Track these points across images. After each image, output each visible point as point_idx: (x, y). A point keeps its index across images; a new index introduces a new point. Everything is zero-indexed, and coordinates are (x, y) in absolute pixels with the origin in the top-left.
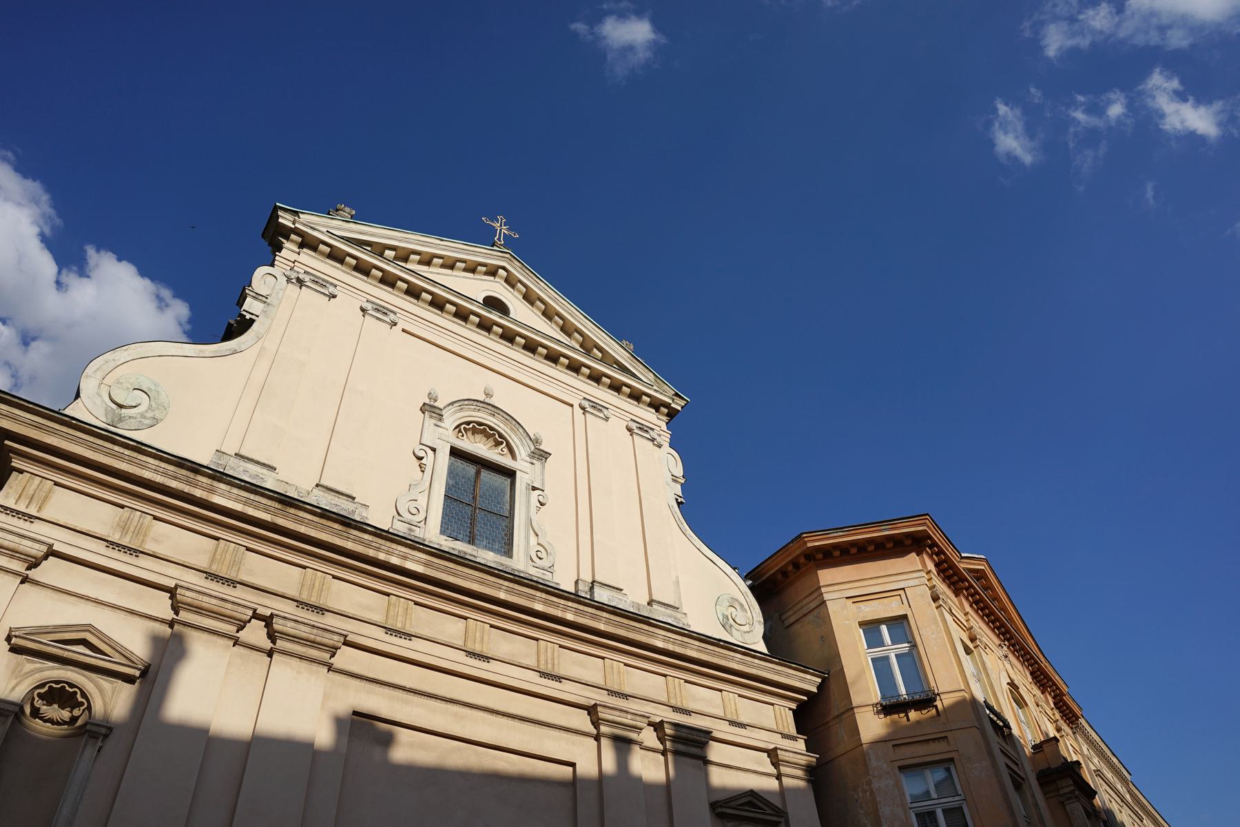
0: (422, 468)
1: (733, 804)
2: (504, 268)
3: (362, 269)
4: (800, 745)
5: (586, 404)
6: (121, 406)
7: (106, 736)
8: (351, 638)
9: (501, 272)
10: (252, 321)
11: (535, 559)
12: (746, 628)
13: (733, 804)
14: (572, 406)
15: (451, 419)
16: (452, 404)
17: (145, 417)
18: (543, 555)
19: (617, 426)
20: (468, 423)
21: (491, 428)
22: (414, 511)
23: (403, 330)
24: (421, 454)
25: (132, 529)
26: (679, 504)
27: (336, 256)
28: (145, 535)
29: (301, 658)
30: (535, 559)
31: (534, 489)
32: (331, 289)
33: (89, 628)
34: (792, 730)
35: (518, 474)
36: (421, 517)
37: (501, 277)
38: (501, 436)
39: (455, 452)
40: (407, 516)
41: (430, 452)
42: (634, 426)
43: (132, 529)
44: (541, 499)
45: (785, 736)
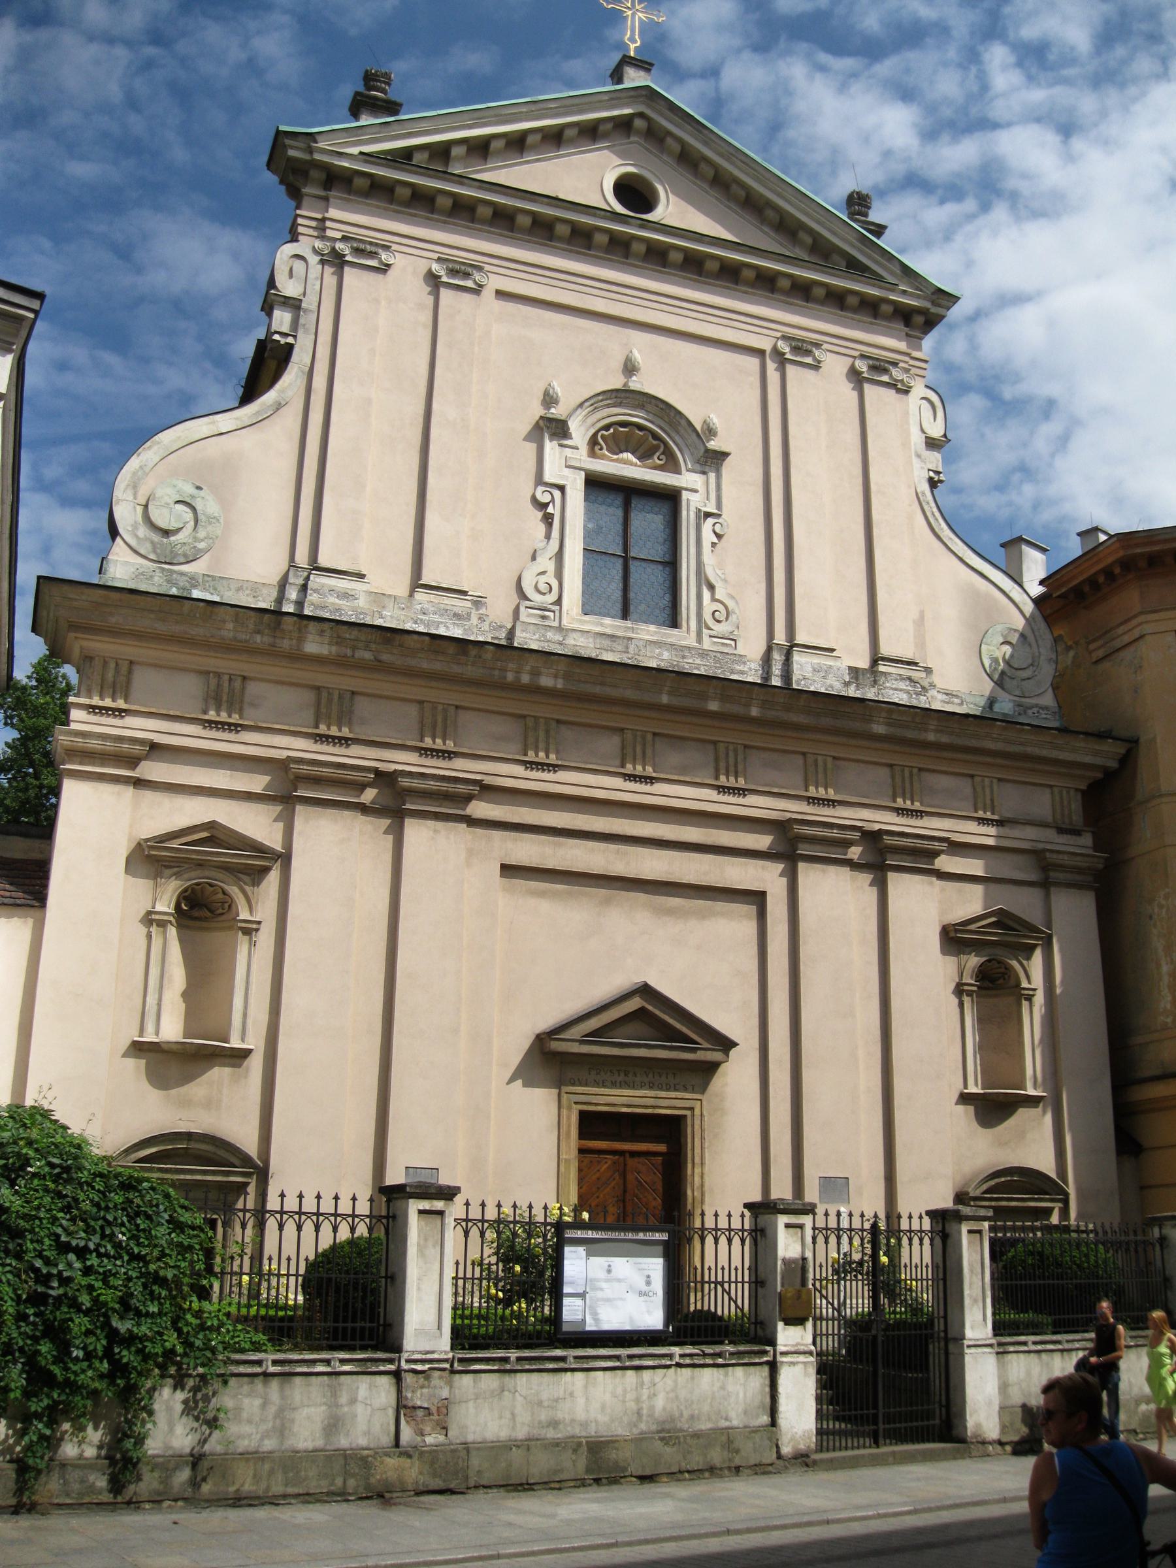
0: (548, 519)
1: (972, 927)
2: (641, 115)
3: (421, 203)
4: (1087, 840)
5: (784, 347)
6: (166, 533)
7: (257, 930)
8: (488, 780)
9: (639, 123)
10: (290, 347)
11: (711, 622)
12: (1025, 674)
13: (972, 927)
14: (760, 353)
15: (580, 430)
16: (581, 405)
17: (196, 539)
18: (721, 616)
19: (835, 366)
20: (607, 428)
21: (640, 427)
22: (543, 587)
23: (501, 294)
24: (546, 498)
25: (225, 698)
26: (933, 484)
27: (379, 192)
28: (242, 701)
29: (437, 816)
30: (711, 622)
31: (708, 515)
32: (384, 256)
33: (212, 825)
34: (1077, 819)
35: (685, 495)
36: (553, 597)
37: (638, 132)
38: (655, 436)
39: (596, 484)
40: (537, 599)
41: (557, 494)
42: (862, 366)
43: (225, 698)
44: (718, 528)
45: (1061, 831)
